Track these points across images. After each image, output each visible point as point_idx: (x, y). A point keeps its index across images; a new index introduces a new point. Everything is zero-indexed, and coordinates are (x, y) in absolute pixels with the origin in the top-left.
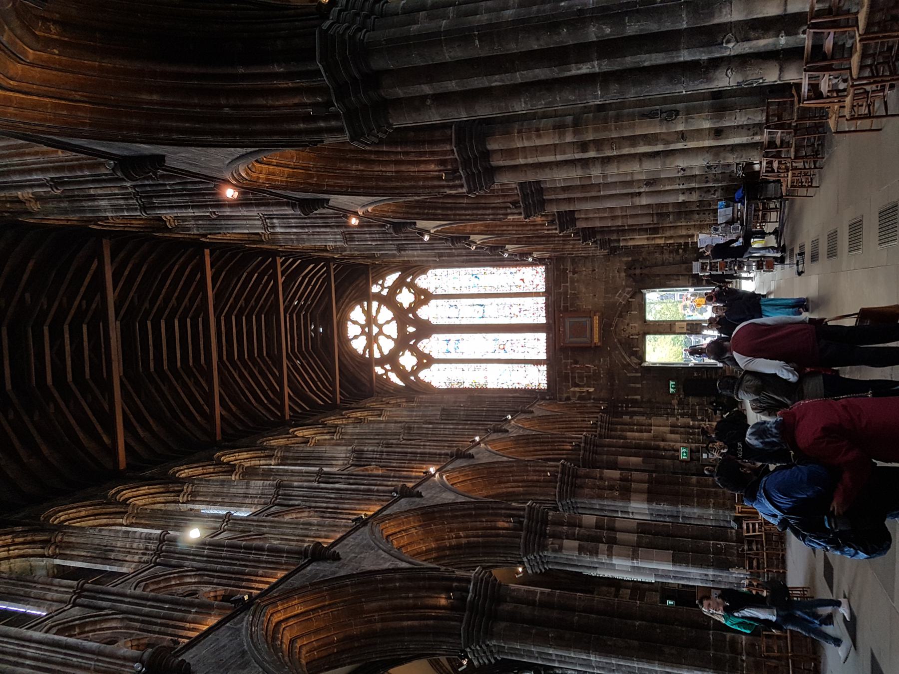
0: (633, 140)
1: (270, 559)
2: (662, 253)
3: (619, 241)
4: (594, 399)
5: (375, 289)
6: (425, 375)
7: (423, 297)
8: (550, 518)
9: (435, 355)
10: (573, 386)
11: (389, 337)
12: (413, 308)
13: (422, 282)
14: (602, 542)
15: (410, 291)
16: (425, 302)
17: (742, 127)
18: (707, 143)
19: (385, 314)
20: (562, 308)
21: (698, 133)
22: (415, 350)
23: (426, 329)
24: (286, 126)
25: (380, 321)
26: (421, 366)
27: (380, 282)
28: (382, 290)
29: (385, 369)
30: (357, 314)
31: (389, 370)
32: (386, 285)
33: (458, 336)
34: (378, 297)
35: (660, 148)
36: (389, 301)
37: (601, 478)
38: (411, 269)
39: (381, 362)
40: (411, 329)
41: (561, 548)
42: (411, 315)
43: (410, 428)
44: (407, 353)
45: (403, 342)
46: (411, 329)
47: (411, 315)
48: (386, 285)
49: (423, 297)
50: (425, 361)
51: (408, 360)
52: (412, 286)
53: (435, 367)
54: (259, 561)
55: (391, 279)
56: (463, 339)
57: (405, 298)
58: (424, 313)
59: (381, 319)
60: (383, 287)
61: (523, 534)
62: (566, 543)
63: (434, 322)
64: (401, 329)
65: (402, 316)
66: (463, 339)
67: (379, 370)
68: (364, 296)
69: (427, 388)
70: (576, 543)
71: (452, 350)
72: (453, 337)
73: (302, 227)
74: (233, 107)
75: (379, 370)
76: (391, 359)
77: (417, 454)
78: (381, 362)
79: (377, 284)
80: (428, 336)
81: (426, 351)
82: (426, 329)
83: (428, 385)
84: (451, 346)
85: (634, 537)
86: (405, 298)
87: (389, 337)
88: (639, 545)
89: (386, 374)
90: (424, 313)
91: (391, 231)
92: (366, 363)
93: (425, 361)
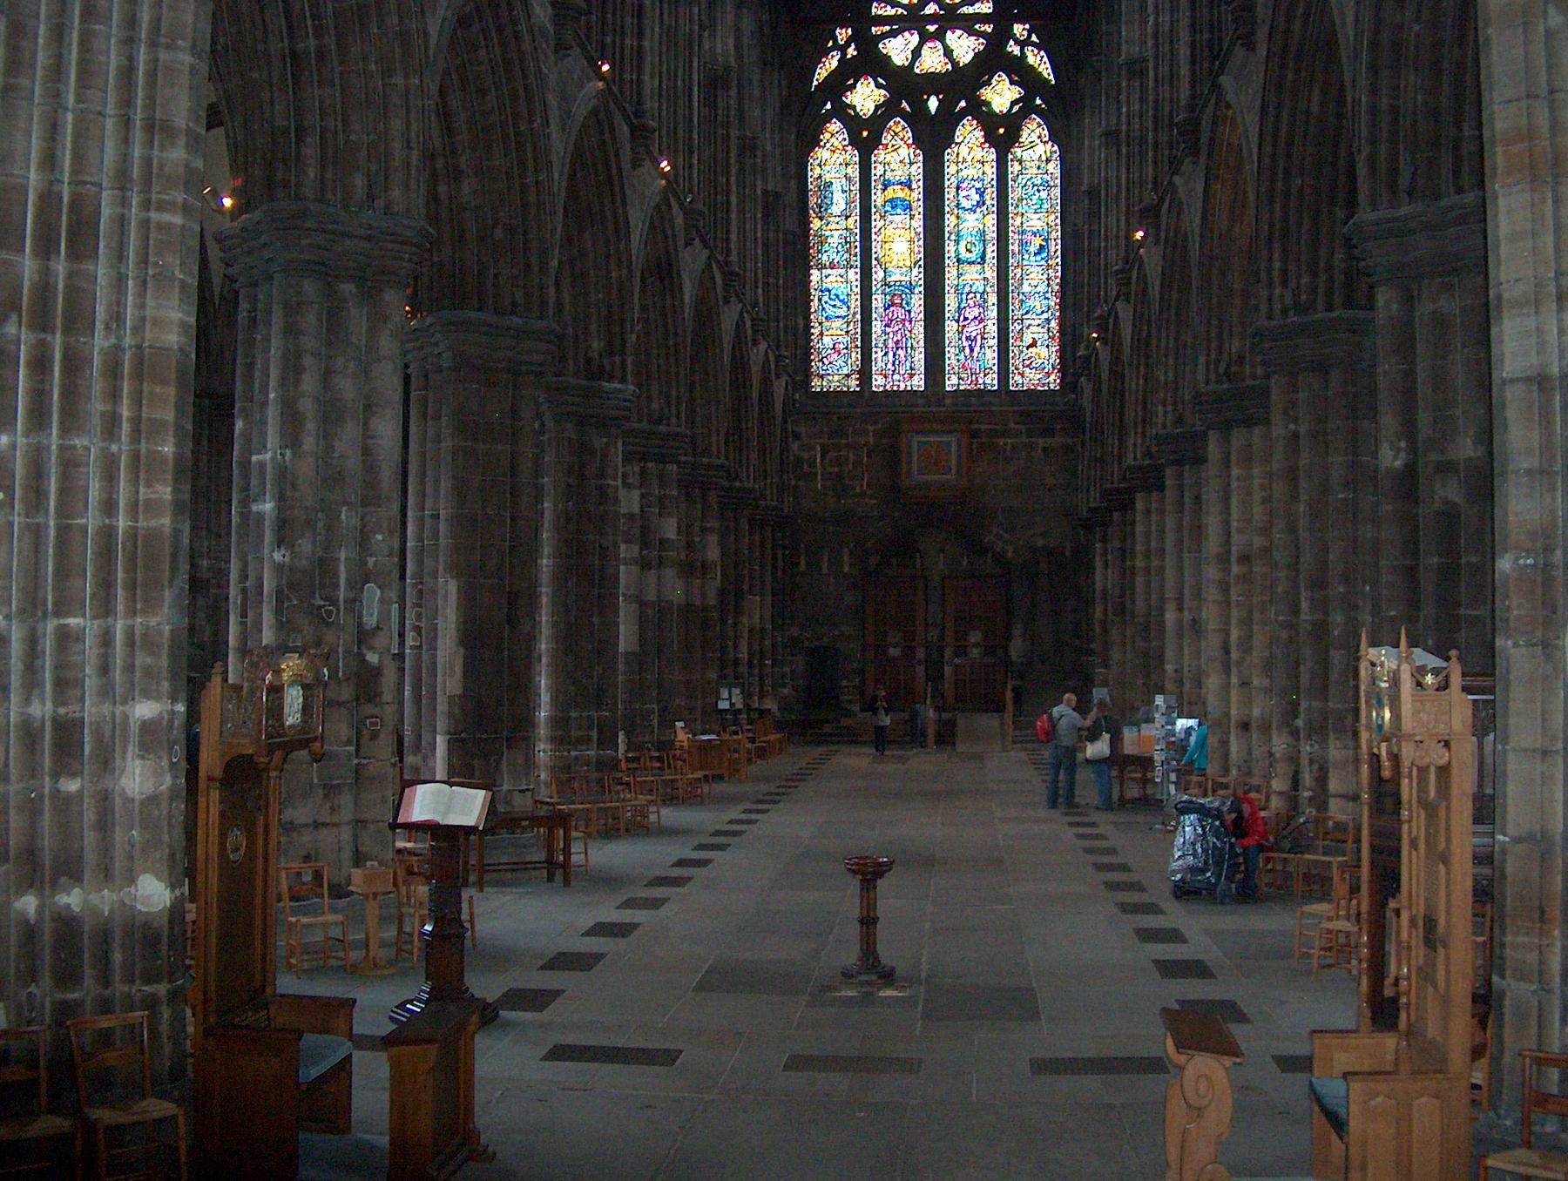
0: (1247, 622)
1: (627, 52)
2: (1075, 611)
3: (1104, 540)
4: (796, 486)
8: (669, 467)
9: (880, 155)
10: (823, 446)
11: (916, 53)
14: (641, 549)
15: (1013, 103)
16: (990, 139)
17: (1250, 753)
18: (1234, 712)
19: (964, 47)
20: (976, 426)
21: (1248, 702)
22: (886, 112)
24: (1277, 245)
25: (951, 37)
26: (853, 123)
27: (1034, 38)
28: (1017, 42)
29: (847, 45)
31: (844, 54)
32: (1029, 51)
33: (919, 208)
34: (1002, 34)
35: (1234, 655)
36: (992, 61)
37: (703, 530)
41: (627, 486)
42: (963, 104)
43: (753, 148)
44: (881, 95)
47: (963, 104)
48: (1029, 51)
50: (866, 137)
51: (865, 97)
52: (1025, 108)
53: (853, 156)
54: (623, 35)
55: (1038, 61)
56: (912, 217)
57: (1001, 95)
58: (969, 134)
60: (1023, 44)
61: (644, 425)
62: (636, 494)
63: (949, 153)
64: (933, 82)
66: (912, 217)
67: (843, 34)
70: (636, 510)
71: (890, 193)
72: (917, 195)
73: (1156, 35)
74: (1301, 190)
76: (871, 63)
77: (639, 74)
79: (1030, 32)
80: (918, 142)
81: (887, 138)
83: (815, 142)
84: (898, 192)
85: (651, 596)
86: (1001, 95)
87: (916, 53)
88: (642, 604)
89: (836, 47)
90: (969, 137)
91: (1146, 202)
93: (866, 137)
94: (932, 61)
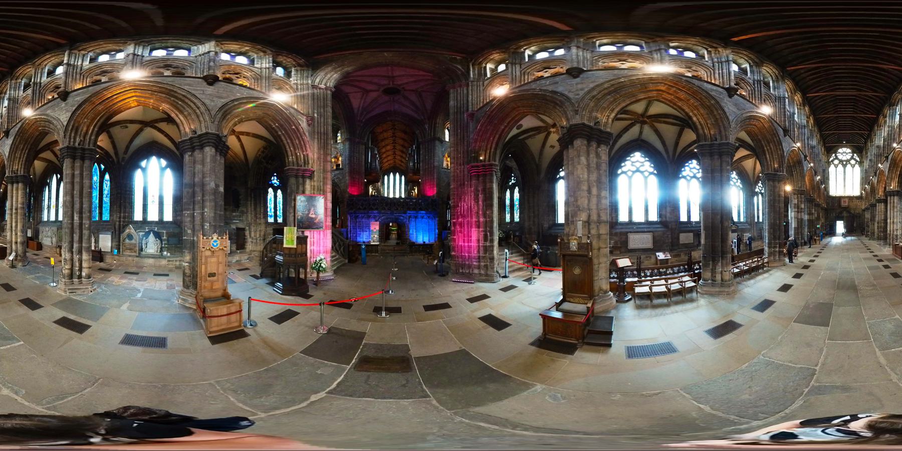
5: (855, 155)
6: (832, 166)
7: (853, 166)
12: (850, 163)
13: (857, 166)
19: (849, 157)
23: (845, 166)
26: (835, 165)
30: (849, 150)
34: (853, 155)
36: (852, 158)
38: (861, 163)
39: (836, 156)
40: (844, 163)
45: (841, 161)
46: (844, 163)
49: (853, 166)
50: (836, 166)
55: (858, 159)
58: (849, 166)
59: (847, 156)
64: (845, 161)
65: (848, 161)
67: (834, 155)
68: (853, 152)
69: (829, 166)
75: (834, 155)
76: (837, 158)
78: (836, 156)
82: (845, 166)
92: (836, 152)
93: (836, 166)
94: (844, 158)
